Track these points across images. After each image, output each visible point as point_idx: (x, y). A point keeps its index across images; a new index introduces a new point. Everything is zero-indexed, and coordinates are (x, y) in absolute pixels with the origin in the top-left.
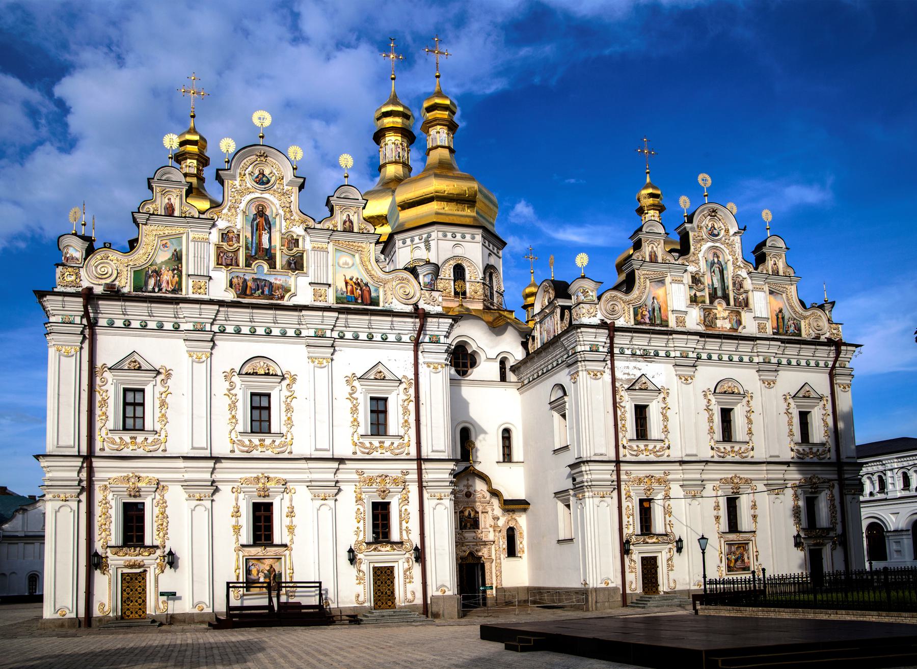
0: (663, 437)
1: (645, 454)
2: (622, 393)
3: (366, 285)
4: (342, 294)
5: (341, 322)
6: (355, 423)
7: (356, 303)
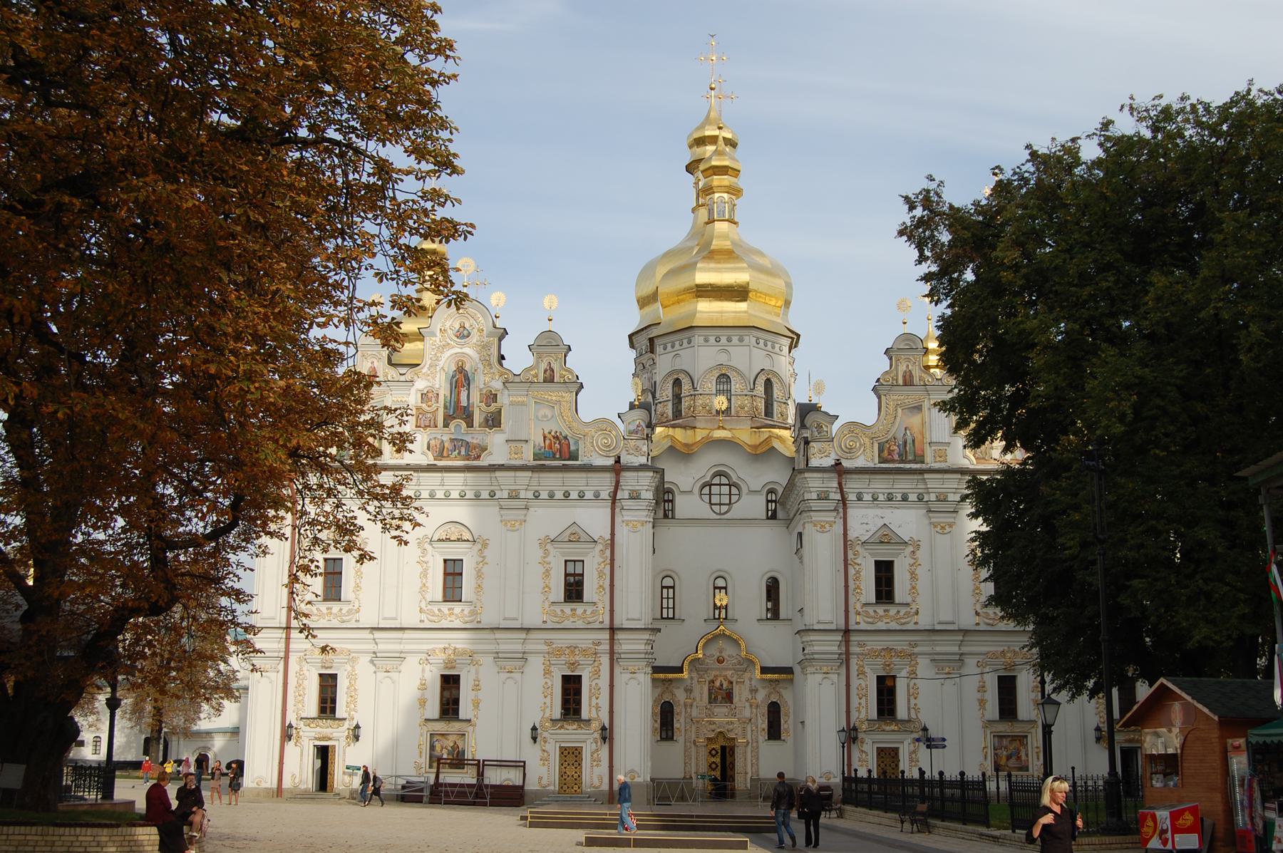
0: (909, 600)
1: (885, 621)
2: (858, 548)
3: (566, 438)
4: (540, 450)
5: (534, 482)
6: (547, 589)
7: (554, 458)
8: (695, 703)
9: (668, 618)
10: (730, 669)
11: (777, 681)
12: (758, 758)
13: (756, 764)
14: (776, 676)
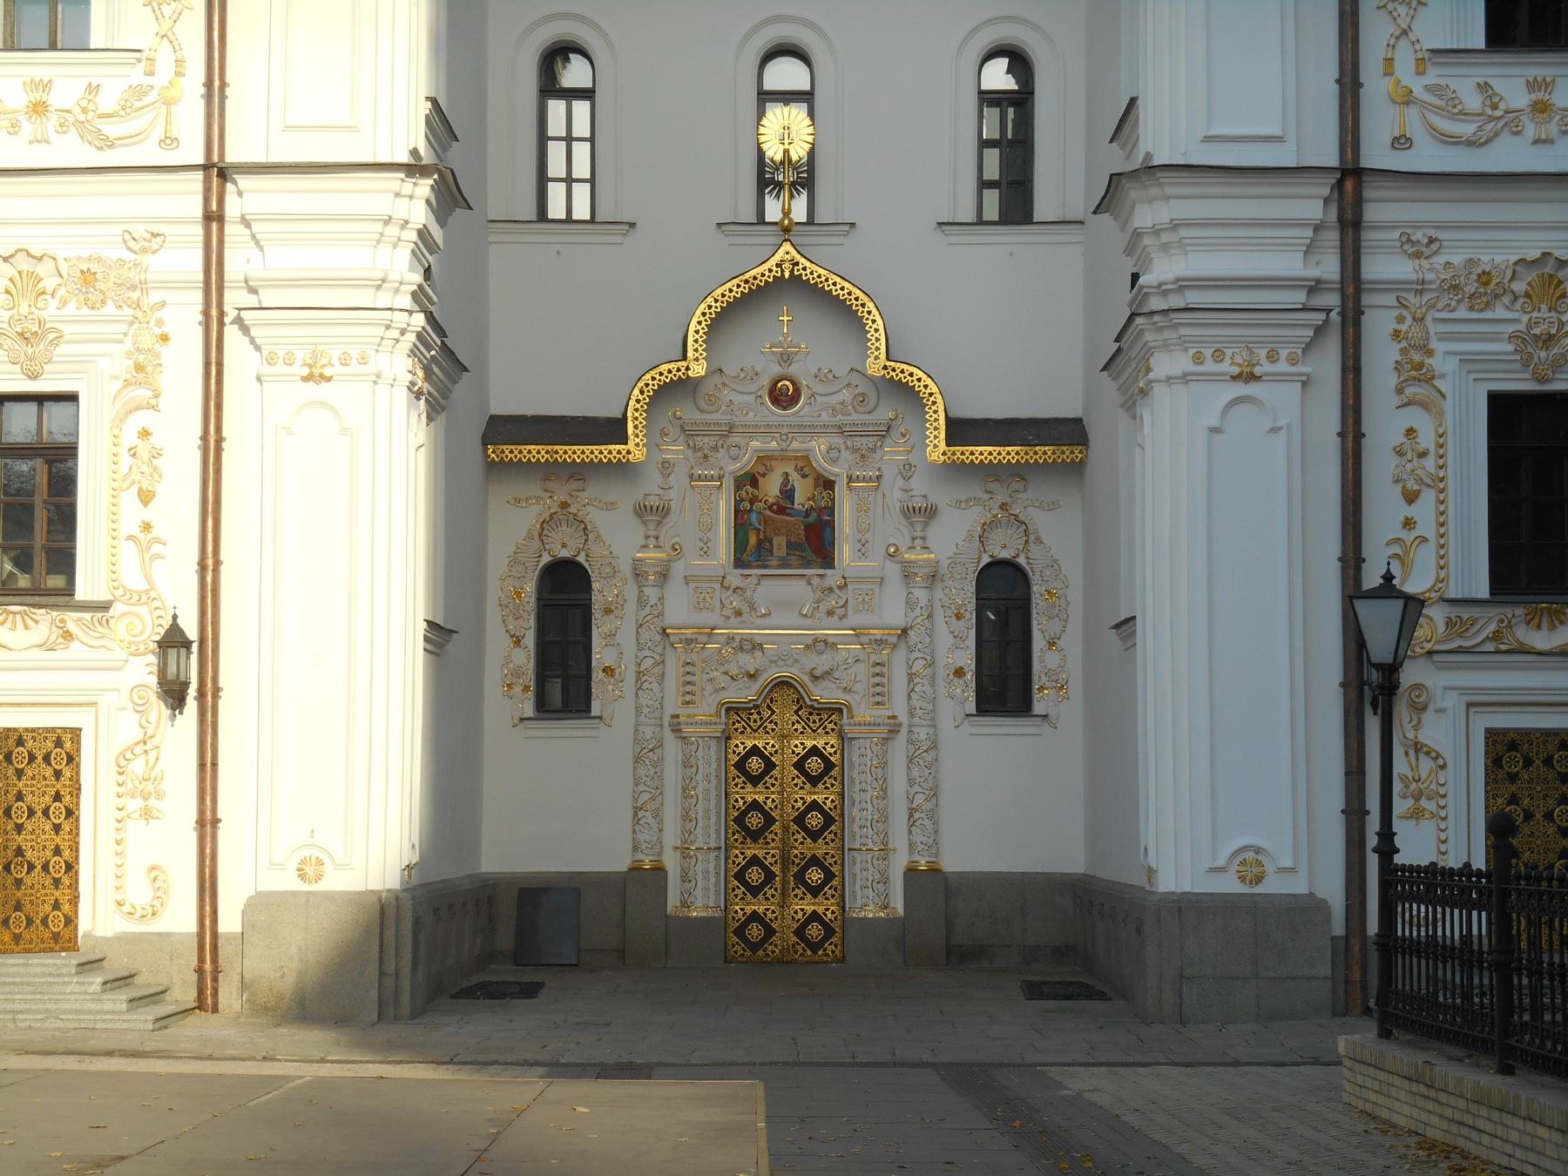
8: (678, 569)
9: (569, 220)
10: (824, 430)
11: (1018, 472)
12: (934, 794)
13: (926, 811)
14: (1010, 453)
